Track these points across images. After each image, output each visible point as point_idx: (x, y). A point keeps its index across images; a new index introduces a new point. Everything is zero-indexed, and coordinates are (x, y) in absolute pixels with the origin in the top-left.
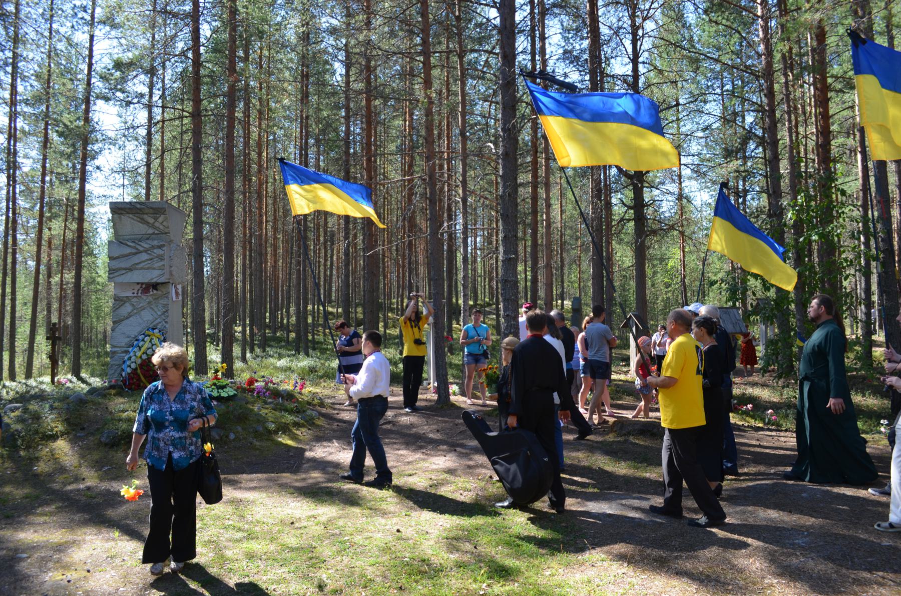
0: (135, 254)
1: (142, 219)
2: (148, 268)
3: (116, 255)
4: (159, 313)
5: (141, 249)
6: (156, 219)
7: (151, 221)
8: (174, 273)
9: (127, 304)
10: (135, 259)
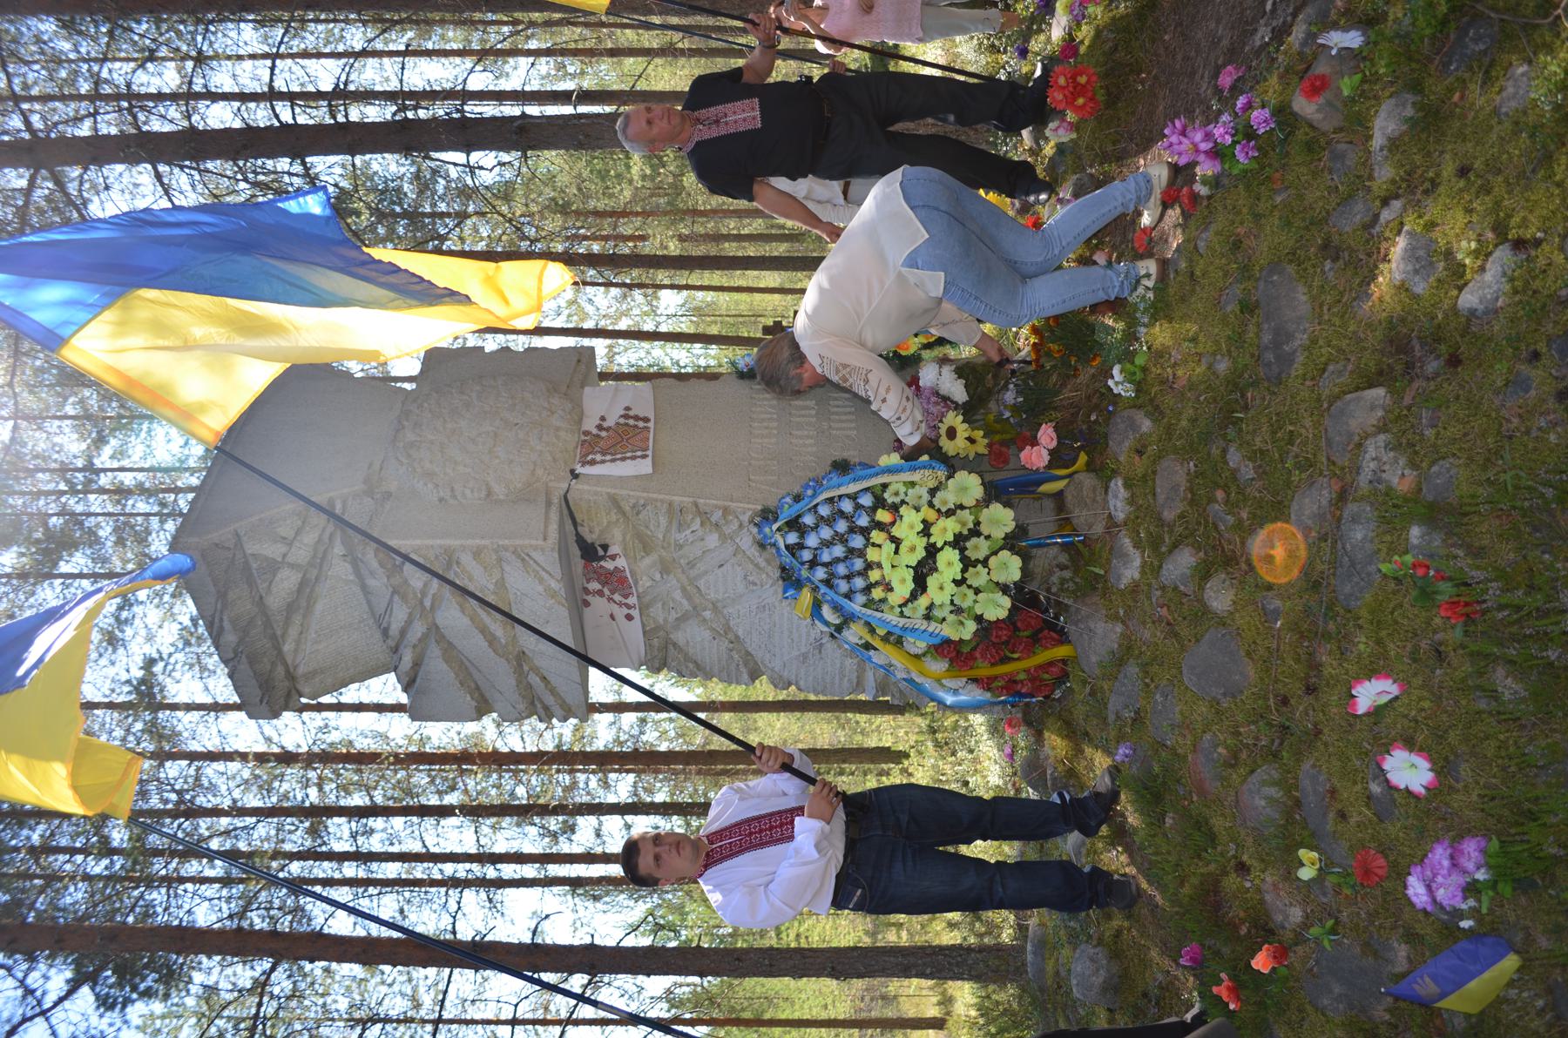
1: (291, 608)
3: (469, 702)
4: (713, 540)
5: (418, 629)
6: (273, 567)
7: (286, 582)
9: (679, 637)
10: (473, 646)
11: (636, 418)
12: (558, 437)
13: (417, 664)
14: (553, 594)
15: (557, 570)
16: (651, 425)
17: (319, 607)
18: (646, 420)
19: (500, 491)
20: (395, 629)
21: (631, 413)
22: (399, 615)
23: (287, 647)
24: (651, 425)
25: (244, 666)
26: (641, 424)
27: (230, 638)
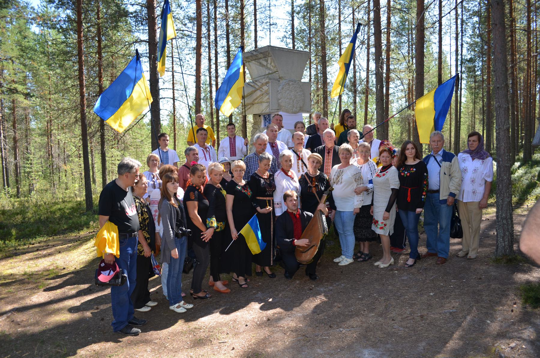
0: (255, 91)
1: (260, 63)
2: (261, 103)
5: (257, 87)
6: (267, 61)
7: (265, 63)
10: (255, 96)
13: (251, 86)
14: (263, 111)
15: (266, 112)
17: (261, 67)
19: (280, 101)
20: (256, 83)
22: (259, 84)
23: (254, 62)
25: (250, 55)
27: (255, 53)
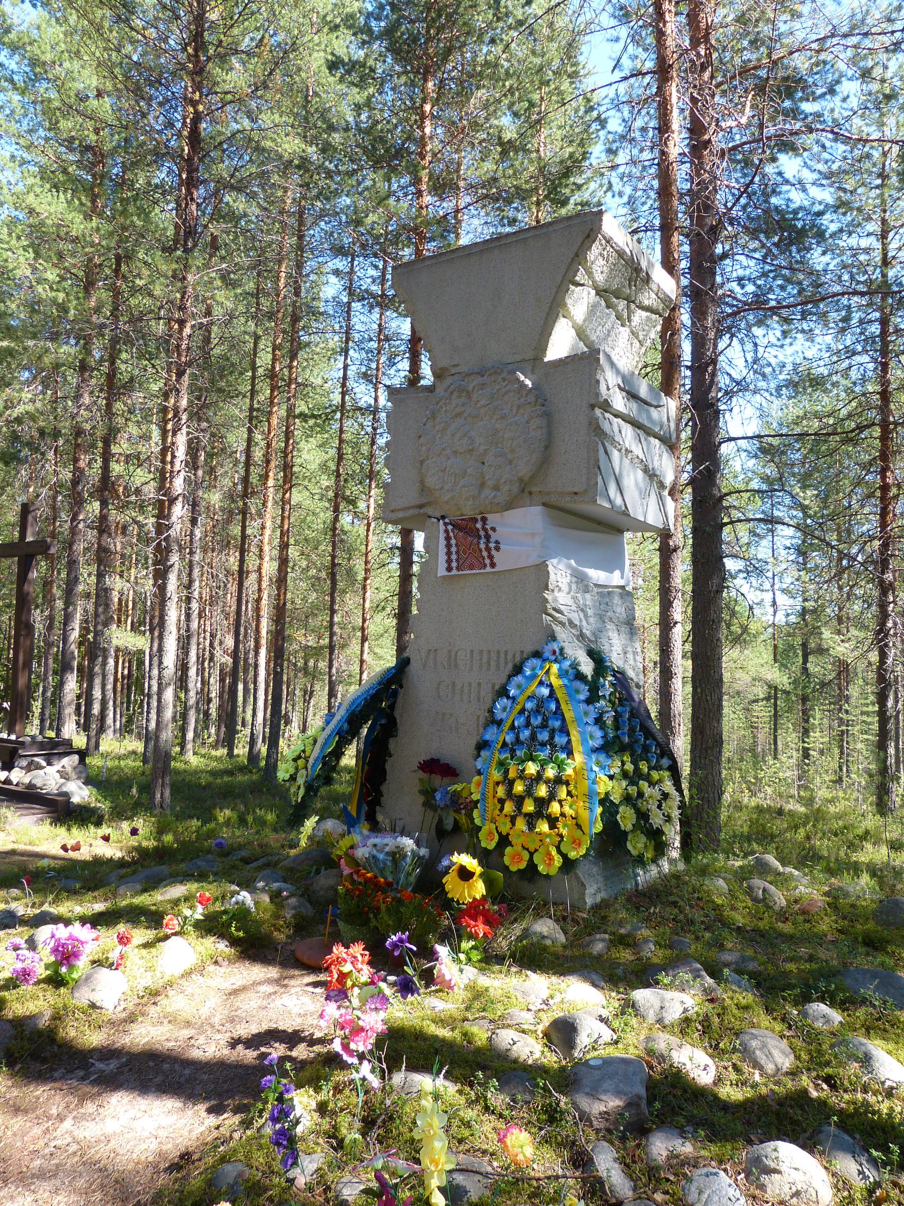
8: (431, 481)
11: (491, 557)
12: (467, 499)
16: (488, 569)
18: (493, 565)
21: (493, 552)
24: (488, 569)
26: (487, 561)
